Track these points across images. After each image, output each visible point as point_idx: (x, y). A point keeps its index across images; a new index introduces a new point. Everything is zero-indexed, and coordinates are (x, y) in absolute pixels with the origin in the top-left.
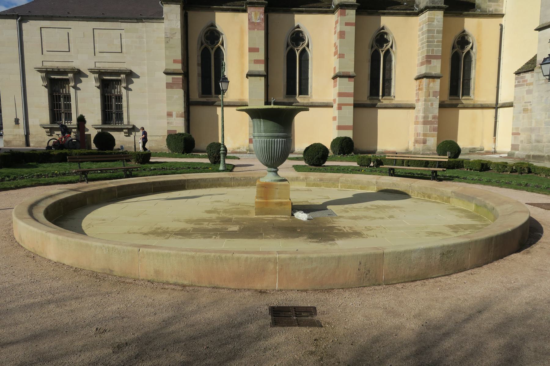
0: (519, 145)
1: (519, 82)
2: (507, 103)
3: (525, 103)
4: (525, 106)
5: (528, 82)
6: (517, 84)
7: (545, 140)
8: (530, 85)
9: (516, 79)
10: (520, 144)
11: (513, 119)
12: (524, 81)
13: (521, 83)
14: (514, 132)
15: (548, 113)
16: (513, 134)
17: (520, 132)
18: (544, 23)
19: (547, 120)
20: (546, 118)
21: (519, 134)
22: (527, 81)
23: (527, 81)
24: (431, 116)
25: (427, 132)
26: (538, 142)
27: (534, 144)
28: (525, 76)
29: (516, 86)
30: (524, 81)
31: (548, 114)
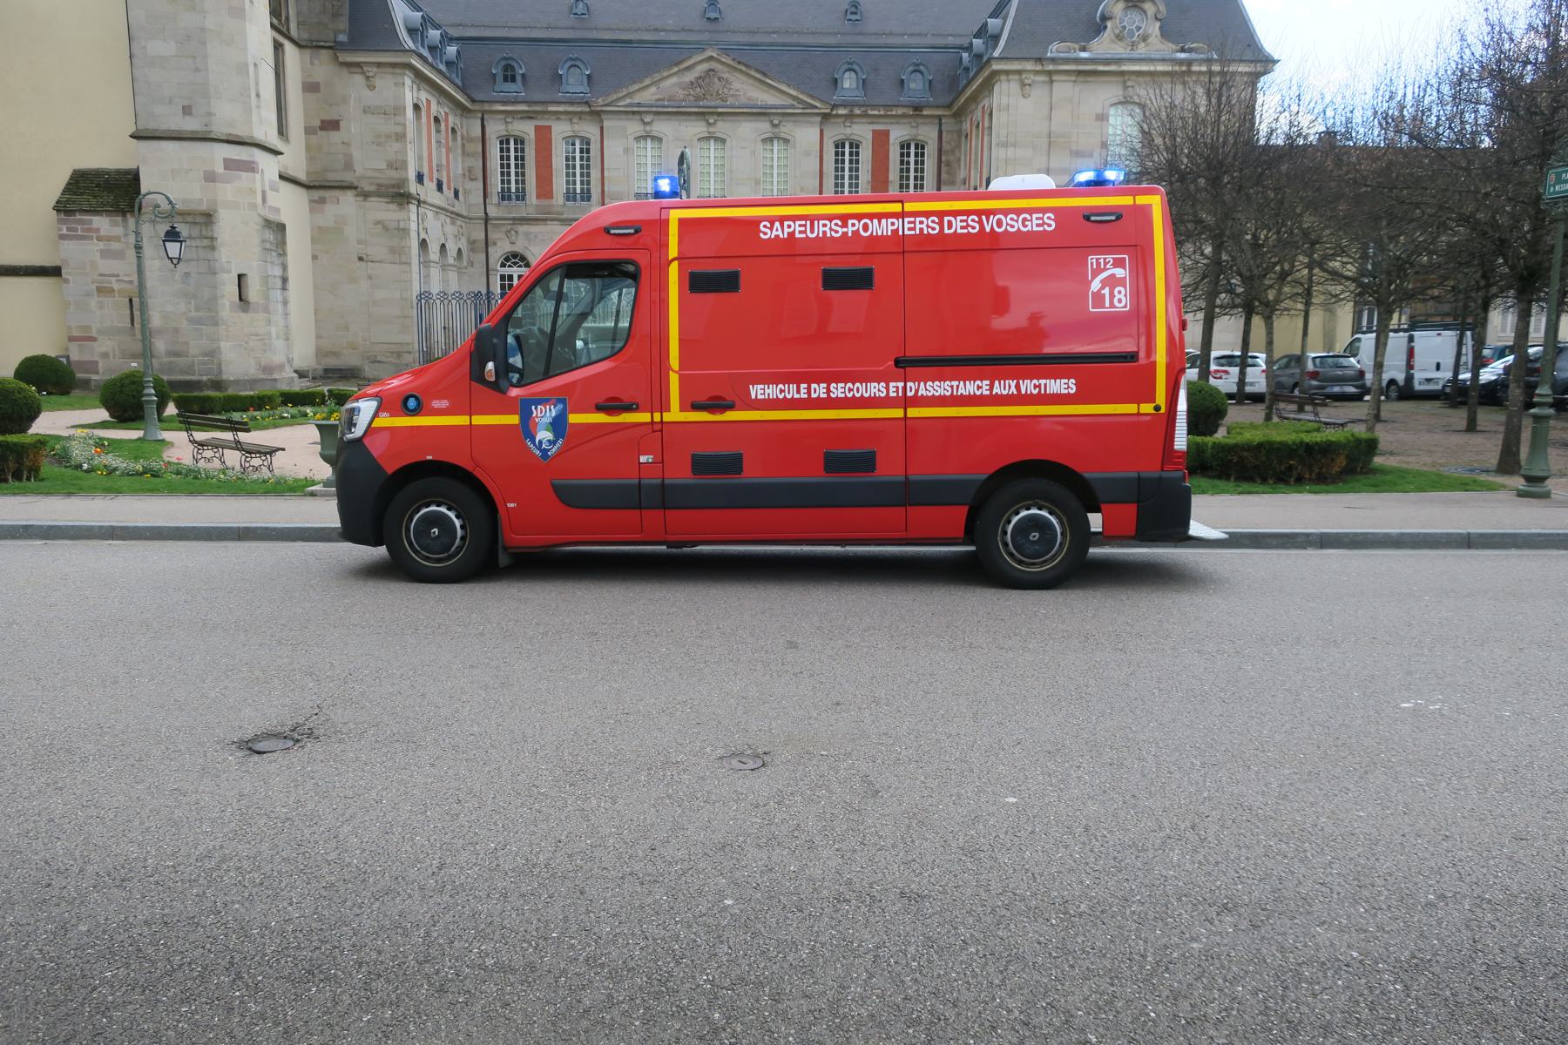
0: (97, 362)
1: (68, 229)
3: (101, 275)
5: (102, 233)
6: (65, 232)
7: (193, 351)
9: (60, 221)
12: (89, 230)
14: (76, 334)
15: (193, 302)
17: (94, 335)
19: (194, 314)
21: (94, 339)
22: (98, 230)
23: (98, 230)
27: (165, 360)
30: (89, 230)
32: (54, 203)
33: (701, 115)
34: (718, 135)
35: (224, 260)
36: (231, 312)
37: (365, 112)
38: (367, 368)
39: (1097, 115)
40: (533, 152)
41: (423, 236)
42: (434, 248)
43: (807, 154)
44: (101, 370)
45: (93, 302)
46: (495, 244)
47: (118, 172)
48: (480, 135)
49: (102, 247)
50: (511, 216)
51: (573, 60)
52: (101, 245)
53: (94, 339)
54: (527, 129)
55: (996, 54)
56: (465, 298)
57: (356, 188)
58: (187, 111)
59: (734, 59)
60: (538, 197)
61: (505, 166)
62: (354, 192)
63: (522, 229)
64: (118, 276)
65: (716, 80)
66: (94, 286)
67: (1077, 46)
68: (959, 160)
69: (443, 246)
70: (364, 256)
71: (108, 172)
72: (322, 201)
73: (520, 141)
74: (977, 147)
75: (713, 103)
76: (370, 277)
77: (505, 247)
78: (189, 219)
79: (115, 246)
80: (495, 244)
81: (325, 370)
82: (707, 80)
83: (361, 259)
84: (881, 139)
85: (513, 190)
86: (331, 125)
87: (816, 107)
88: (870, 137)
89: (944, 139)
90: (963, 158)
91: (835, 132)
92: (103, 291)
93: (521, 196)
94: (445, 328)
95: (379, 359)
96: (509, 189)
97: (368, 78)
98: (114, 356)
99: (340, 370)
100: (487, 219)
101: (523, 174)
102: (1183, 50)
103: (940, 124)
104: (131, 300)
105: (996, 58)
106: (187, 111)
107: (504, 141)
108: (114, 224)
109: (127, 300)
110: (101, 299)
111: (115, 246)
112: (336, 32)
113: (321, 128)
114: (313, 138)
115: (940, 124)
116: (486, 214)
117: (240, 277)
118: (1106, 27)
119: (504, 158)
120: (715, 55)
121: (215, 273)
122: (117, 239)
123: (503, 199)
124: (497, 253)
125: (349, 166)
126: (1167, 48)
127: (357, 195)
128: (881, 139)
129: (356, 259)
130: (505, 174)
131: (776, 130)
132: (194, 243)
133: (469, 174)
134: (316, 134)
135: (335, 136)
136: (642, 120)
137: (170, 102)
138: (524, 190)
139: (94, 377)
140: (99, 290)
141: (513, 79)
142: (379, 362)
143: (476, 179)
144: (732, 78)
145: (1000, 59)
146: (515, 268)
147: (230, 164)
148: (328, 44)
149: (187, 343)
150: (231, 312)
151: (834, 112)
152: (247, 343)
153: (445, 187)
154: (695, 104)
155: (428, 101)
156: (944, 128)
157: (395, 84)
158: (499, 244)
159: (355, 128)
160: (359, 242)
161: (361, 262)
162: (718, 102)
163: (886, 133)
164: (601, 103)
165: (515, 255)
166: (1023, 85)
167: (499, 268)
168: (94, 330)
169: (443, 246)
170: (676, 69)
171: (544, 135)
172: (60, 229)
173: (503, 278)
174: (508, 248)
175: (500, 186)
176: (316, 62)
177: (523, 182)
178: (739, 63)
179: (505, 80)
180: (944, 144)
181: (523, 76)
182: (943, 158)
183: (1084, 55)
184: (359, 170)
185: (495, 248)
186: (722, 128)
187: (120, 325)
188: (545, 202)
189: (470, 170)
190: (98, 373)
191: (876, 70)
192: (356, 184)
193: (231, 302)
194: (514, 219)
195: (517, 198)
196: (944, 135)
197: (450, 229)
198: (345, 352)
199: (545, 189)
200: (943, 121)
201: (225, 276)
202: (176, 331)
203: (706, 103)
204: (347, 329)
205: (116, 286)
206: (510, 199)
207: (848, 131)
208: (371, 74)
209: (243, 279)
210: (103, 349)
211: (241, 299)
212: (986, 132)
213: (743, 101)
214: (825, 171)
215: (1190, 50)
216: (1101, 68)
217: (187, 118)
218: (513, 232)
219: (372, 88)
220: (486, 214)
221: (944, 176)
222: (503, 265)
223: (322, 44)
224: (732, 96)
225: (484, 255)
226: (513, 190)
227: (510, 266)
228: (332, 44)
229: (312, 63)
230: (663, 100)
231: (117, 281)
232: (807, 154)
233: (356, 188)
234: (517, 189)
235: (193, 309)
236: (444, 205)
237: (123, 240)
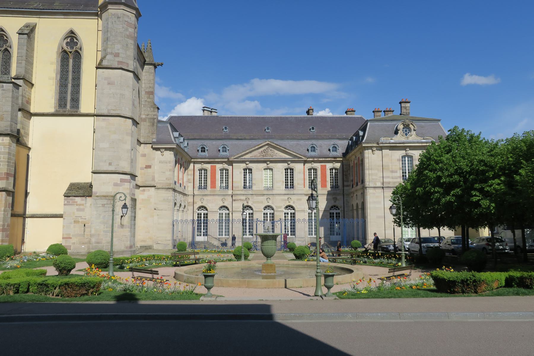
1: (67, 202)
2: (37, 214)
3: (76, 217)
4: (76, 219)
5: (78, 203)
6: (66, 203)
8: (80, 205)
9: (65, 200)
10: (72, 245)
12: (74, 202)
13: (71, 203)
14: (65, 236)
15: (106, 225)
17: (71, 237)
18: (98, 169)
20: (104, 228)
21: (70, 238)
22: (77, 202)
24: (6, 224)
25: (3, 239)
26: (98, 243)
27: (94, 245)
28: (75, 199)
29: (65, 205)
30: (74, 202)
32: (63, 194)
33: (265, 162)
34: (270, 167)
35: (117, 211)
36: (118, 228)
37: (160, 162)
38: (155, 246)
39: (398, 159)
40: (210, 174)
41: (175, 201)
42: (178, 205)
43: (300, 173)
44: (72, 249)
46: (196, 203)
47: (85, 183)
48: (193, 169)
50: (202, 194)
51: (224, 145)
52: (77, 207)
53: (70, 238)
54: (208, 166)
55: (364, 141)
56: (189, 221)
57: (155, 187)
58: (110, 164)
59: (275, 144)
60: (211, 188)
61: (200, 178)
63: (205, 198)
64: (81, 217)
65: (270, 150)
66: (73, 221)
67: (389, 138)
68: (350, 174)
69: (181, 204)
71: (81, 184)
72: (144, 191)
73: (206, 170)
74: (357, 169)
75: (268, 158)
77: (200, 204)
78: (107, 198)
79: (82, 207)
80: (196, 203)
81: (141, 247)
82: (267, 150)
83: (155, 209)
84: (323, 169)
85: (203, 186)
86: (148, 167)
87: (302, 158)
88: (320, 167)
89: (344, 167)
90: (351, 173)
91: (308, 166)
92: (76, 222)
93: (205, 187)
94: (179, 231)
95: (159, 242)
96: (202, 185)
97: (161, 152)
98: (77, 244)
99: (146, 246)
100: (194, 196)
101: (206, 181)
102: (424, 139)
103: (343, 163)
105: (364, 143)
106: (110, 164)
107: (200, 170)
108: (83, 200)
109: (84, 225)
110: (75, 225)
111: (82, 207)
112: (153, 139)
113: (145, 168)
114: (143, 171)
115: (343, 163)
116: (194, 193)
118: (398, 133)
119: (200, 175)
120: (269, 143)
122: (83, 205)
123: (199, 188)
124: (196, 206)
125: (153, 179)
126: (419, 139)
127: (155, 189)
128: (323, 169)
129: (154, 209)
130: (200, 181)
131: (289, 165)
132: (108, 206)
133: (188, 181)
134: (144, 169)
135: (149, 169)
136: (246, 163)
137: (105, 162)
138: (206, 186)
140: (75, 222)
141: (204, 151)
143: (191, 183)
144: (274, 150)
145: (365, 143)
146: (202, 211)
147: (122, 180)
148: (150, 142)
149: (102, 239)
150: (118, 228)
151: (308, 160)
152: (122, 239)
153: (182, 185)
154: (262, 158)
155: (179, 159)
156: (344, 164)
157: (170, 154)
158: (197, 203)
159: (156, 167)
161: (155, 210)
162: (271, 157)
163: (325, 166)
164: (233, 158)
165: (203, 207)
166: (373, 151)
167: (197, 211)
168: (71, 235)
169: (181, 204)
170: (257, 147)
171: (213, 170)
172: (64, 202)
173: (198, 214)
174: (201, 204)
175: (198, 184)
176: (146, 148)
177: (206, 183)
178: (277, 145)
179: (202, 151)
180: (344, 169)
181: (207, 150)
182: (344, 173)
183: (392, 141)
184: (157, 180)
185: (196, 205)
186: (271, 165)
187: (80, 233)
188: (213, 189)
189: (189, 180)
190: (71, 250)
191: (321, 146)
192: (155, 185)
193: (118, 225)
194: (203, 195)
195: (204, 188)
196: (344, 166)
197: (182, 199)
198: (147, 240)
199: (213, 185)
200: (343, 162)
201: (117, 216)
202: (99, 235)
203: (266, 158)
205: (80, 220)
206: (201, 188)
207: (313, 165)
208: (162, 151)
210: (74, 241)
212: (360, 165)
213: (278, 157)
214: (305, 178)
215: (426, 139)
216: (398, 145)
217: (110, 166)
218: (202, 199)
219: (163, 155)
220: (194, 193)
221: (345, 179)
222: (198, 210)
223: (148, 142)
224: (275, 155)
225: (193, 207)
226: (203, 186)
227: (201, 210)
228: (151, 142)
229: (144, 148)
230: (253, 157)
232: (300, 173)
233: (155, 187)
234: (204, 185)
236: (182, 191)
237: (84, 205)
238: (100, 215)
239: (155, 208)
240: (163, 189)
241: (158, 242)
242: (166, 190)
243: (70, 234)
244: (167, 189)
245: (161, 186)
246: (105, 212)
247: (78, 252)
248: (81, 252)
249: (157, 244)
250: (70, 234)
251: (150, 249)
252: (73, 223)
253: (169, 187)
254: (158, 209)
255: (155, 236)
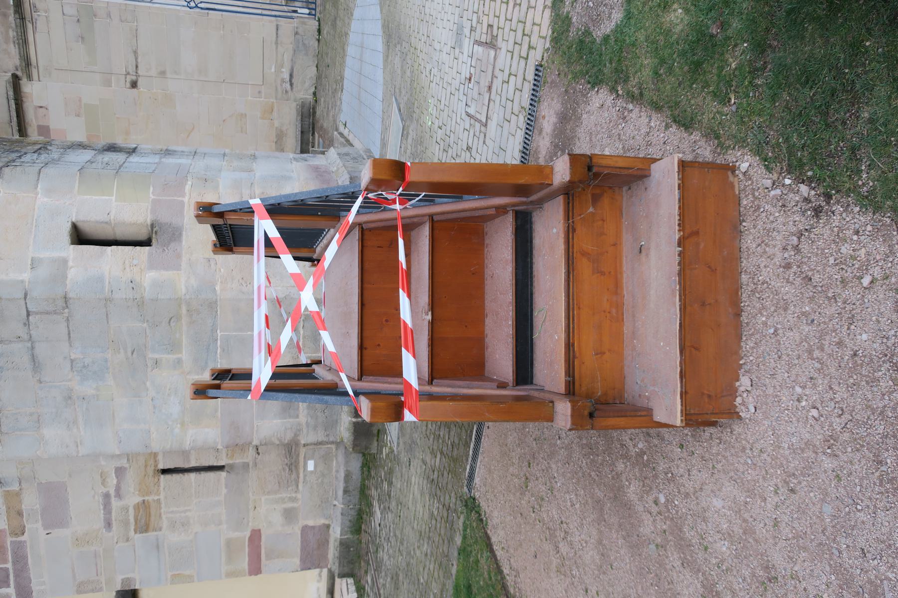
0: (305, 529)
3: (108, 525)
4: (126, 523)
8: (20, 514)
10: (302, 522)
11: (189, 579)
13: (9, 565)
16: (255, 569)
17: (248, 534)
19: (185, 355)
20: (179, 361)
21: (256, 536)
31: (156, 356)
35: (26, 276)
36: (178, 268)
44: (322, 521)
45: (172, 538)
49: (39, 525)
52: (34, 528)
53: (256, 536)
57: (16, 79)
62: (24, 81)
64: (107, 496)
70: (129, 78)
76: (163, 73)
83: (134, 85)
95: (286, 76)
99: (302, 132)
104: (165, 471)
110: (165, 524)
111: (30, 501)
117: (80, 237)
121: (66, 299)
127: (30, 78)
139: (336, 533)
140: (144, 527)
142: (291, 76)
150: (178, 268)
160: (108, 83)
161: (139, 83)
168: (237, 534)
187: (224, 491)
190: (328, 526)
193: (152, 266)
198: (277, 124)
201: (74, 274)
204: (243, 116)
205: (132, 499)
209: (90, 229)
210: (277, 518)
211: (147, 243)
231: (118, 495)
235: (172, 357)
238: (69, 398)
239: (128, 85)
240: (25, 42)
241: (283, 81)
242: (29, 26)
243: (229, 543)
244: (22, 18)
245: (14, 50)
246: (36, 364)
247: (346, 491)
248: (348, 476)
249: (291, 85)
250: (229, 543)
251: (314, 113)
252: (151, 535)
253: (12, 11)
254: (132, 69)
255: (260, 92)
